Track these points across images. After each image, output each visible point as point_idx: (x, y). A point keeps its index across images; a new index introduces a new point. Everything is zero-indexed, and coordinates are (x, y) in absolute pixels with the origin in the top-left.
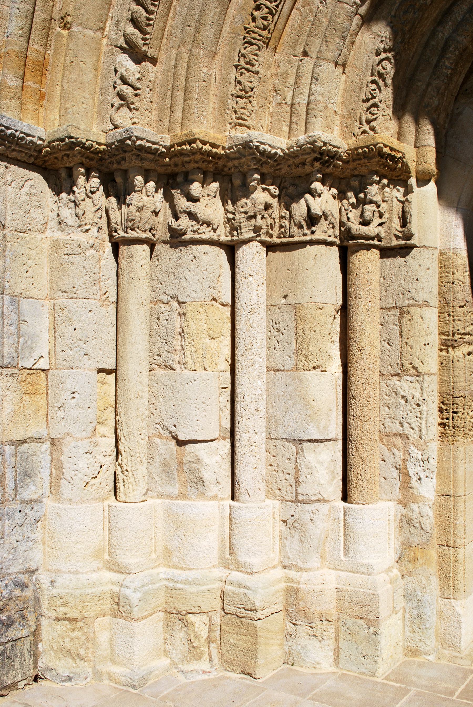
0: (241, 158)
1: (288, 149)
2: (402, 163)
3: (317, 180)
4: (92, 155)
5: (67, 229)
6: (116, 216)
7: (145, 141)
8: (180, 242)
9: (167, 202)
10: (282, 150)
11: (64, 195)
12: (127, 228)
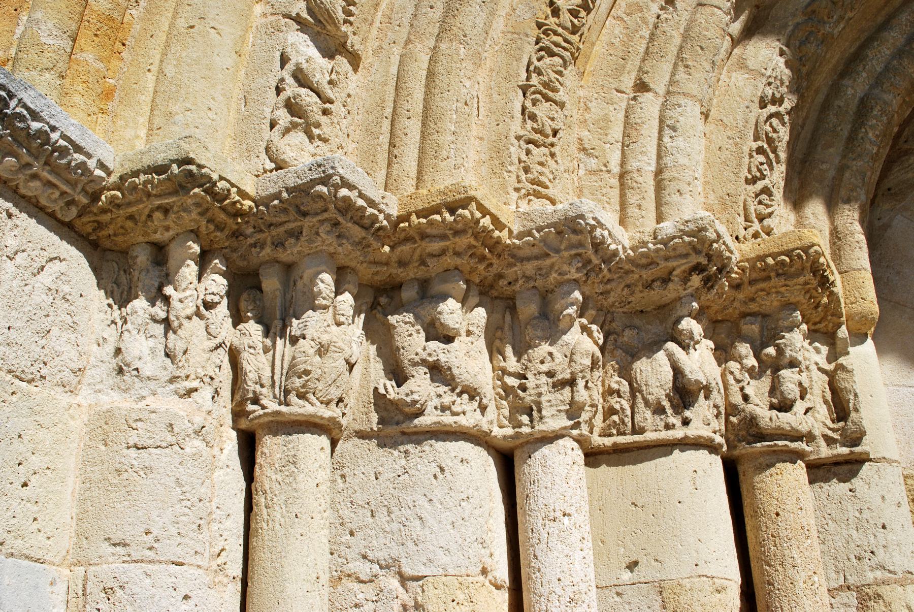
0: (548, 255)
1: (631, 249)
2: (828, 297)
4: (222, 216)
5: (138, 384)
6: (256, 365)
7: (356, 193)
8: (403, 433)
9: (373, 343)
10: (624, 248)
11: (140, 304)
12: (287, 392)
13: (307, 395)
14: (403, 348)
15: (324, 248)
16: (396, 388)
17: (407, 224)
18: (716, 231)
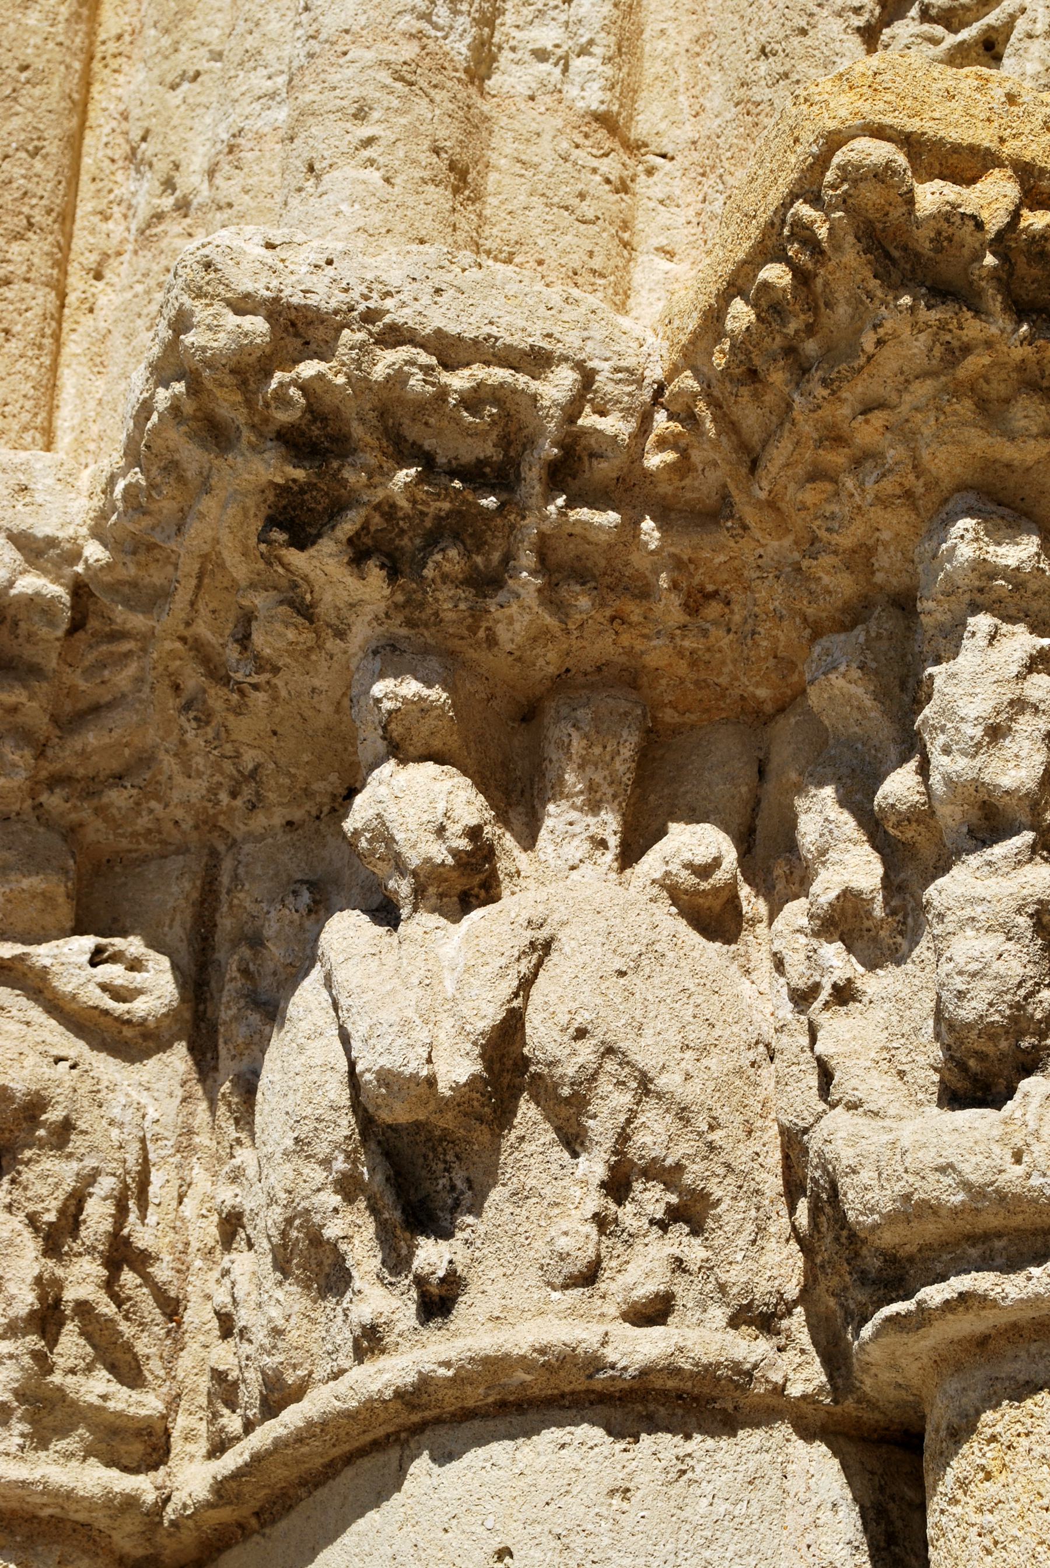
1: (97, 534)
3: (400, 751)
18: (242, 305)
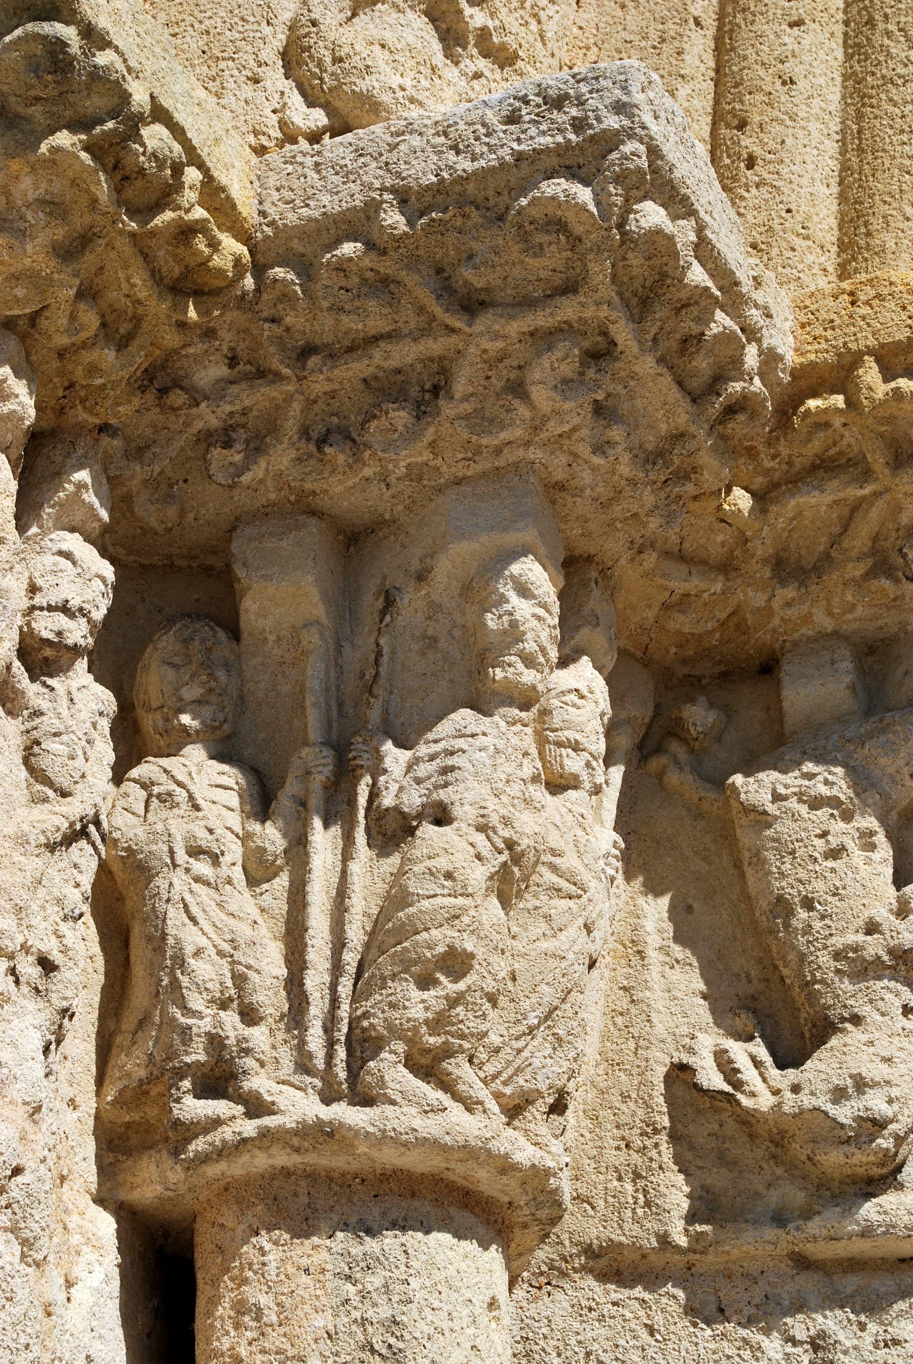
6: (221, 927)
8: (802, 1263)
9: (653, 888)
12: (363, 1045)
13: (449, 1065)
14: (808, 904)
15: (535, 454)
16: (774, 1072)
17: (839, 400)
